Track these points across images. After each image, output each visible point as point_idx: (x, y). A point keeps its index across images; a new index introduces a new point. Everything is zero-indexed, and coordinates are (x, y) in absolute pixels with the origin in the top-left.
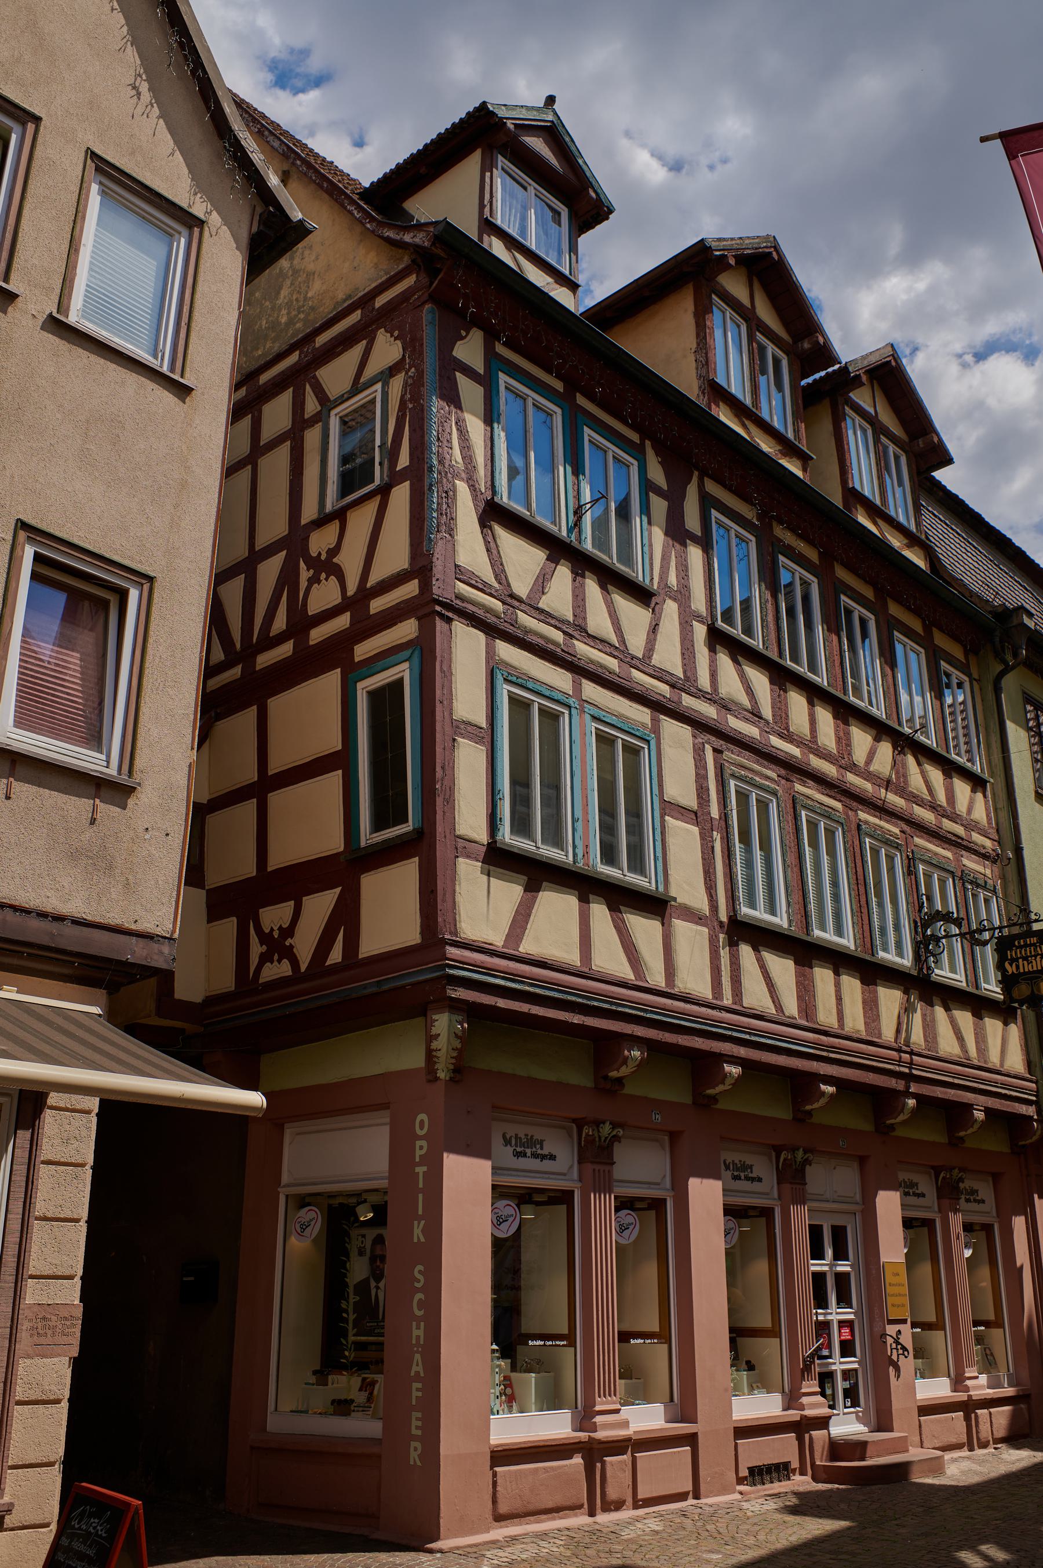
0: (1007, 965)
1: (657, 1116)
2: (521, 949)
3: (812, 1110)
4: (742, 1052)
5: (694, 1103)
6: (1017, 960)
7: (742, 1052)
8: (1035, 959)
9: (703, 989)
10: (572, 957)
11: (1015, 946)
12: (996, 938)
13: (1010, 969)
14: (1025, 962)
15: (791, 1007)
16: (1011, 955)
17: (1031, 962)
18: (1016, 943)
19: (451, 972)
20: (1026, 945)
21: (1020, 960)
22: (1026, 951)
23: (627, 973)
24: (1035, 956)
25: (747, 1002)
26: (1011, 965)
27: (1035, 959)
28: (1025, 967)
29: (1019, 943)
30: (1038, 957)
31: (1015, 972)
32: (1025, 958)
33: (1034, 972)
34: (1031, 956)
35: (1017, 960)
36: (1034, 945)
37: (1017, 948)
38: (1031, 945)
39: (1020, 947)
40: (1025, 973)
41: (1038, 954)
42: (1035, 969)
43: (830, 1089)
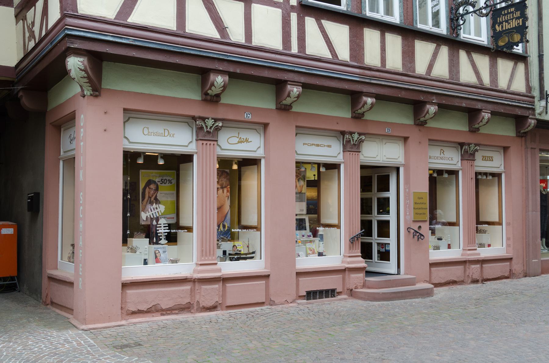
0: (497, 26)
1: (248, 115)
2: (128, 21)
3: (364, 112)
4: (303, 79)
5: (276, 109)
6: (502, 23)
7: (303, 79)
8: (512, 21)
9: (277, 44)
10: (171, 25)
11: (502, 14)
12: (492, 11)
13: (498, 29)
14: (507, 24)
15: (344, 54)
16: (499, 20)
17: (510, 23)
18: (503, 13)
19: (69, 33)
20: (508, 13)
21: (504, 23)
22: (507, 16)
23: (214, 34)
24: (512, 19)
25: (310, 50)
26: (499, 26)
27: (512, 21)
28: (506, 26)
29: (504, 12)
30: (514, 20)
31: (501, 30)
32: (507, 21)
33: (511, 29)
34: (510, 20)
35: (501, 23)
36: (512, 12)
37: (503, 15)
38: (511, 12)
39: (505, 15)
40: (506, 30)
41: (514, 18)
42: (512, 27)
43: (370, 100)
